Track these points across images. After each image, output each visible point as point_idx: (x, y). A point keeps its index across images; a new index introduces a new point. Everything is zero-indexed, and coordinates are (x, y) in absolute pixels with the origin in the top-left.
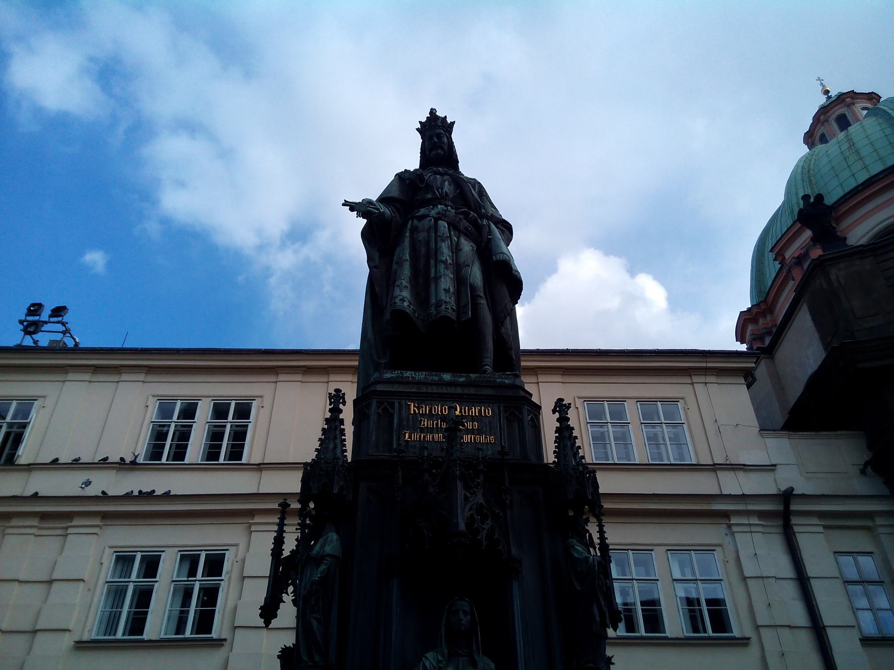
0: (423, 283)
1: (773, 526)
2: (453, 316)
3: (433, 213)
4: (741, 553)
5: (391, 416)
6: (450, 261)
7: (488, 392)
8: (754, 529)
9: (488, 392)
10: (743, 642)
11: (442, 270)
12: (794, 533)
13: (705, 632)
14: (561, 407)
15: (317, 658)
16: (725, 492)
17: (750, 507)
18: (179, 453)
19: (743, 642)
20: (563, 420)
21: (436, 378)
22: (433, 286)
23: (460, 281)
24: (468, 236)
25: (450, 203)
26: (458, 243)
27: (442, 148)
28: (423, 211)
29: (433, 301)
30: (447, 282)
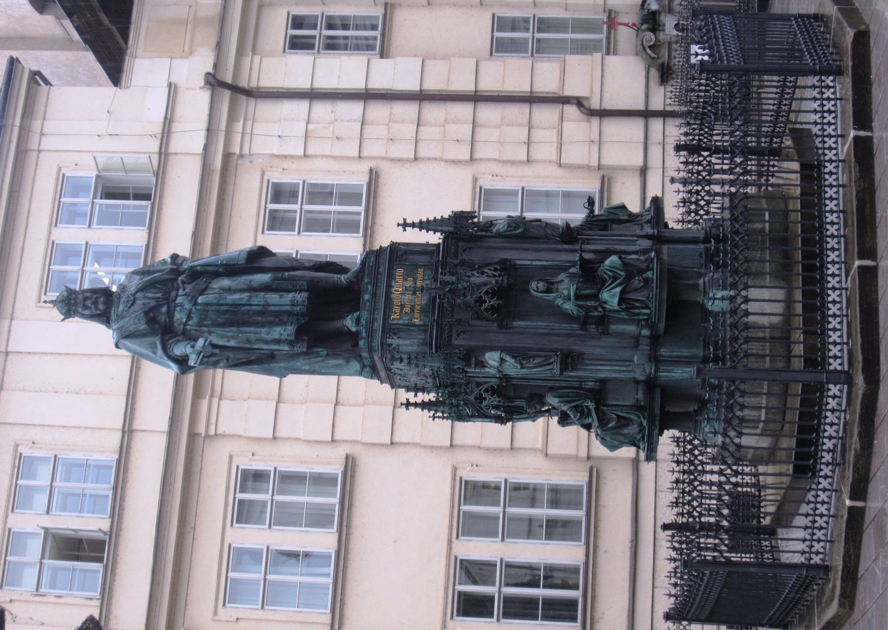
1: (247, 107)
2: (305, 295)
3: (188, 306)
4: (275, 152)
6: (247, 294)
8: (248, 130)
10: (374, 177)
12: (258, 88)
13: (360, 214)
14: (405, 225)
15: (552, 360)
16: (199, 149)
17: (223, 126)
19: (374, 177)
20: (413, 225)
22: (272, 308)
23: (266, 288)
25: (174, 294)
27: (97, 298)
30: (273, 298)
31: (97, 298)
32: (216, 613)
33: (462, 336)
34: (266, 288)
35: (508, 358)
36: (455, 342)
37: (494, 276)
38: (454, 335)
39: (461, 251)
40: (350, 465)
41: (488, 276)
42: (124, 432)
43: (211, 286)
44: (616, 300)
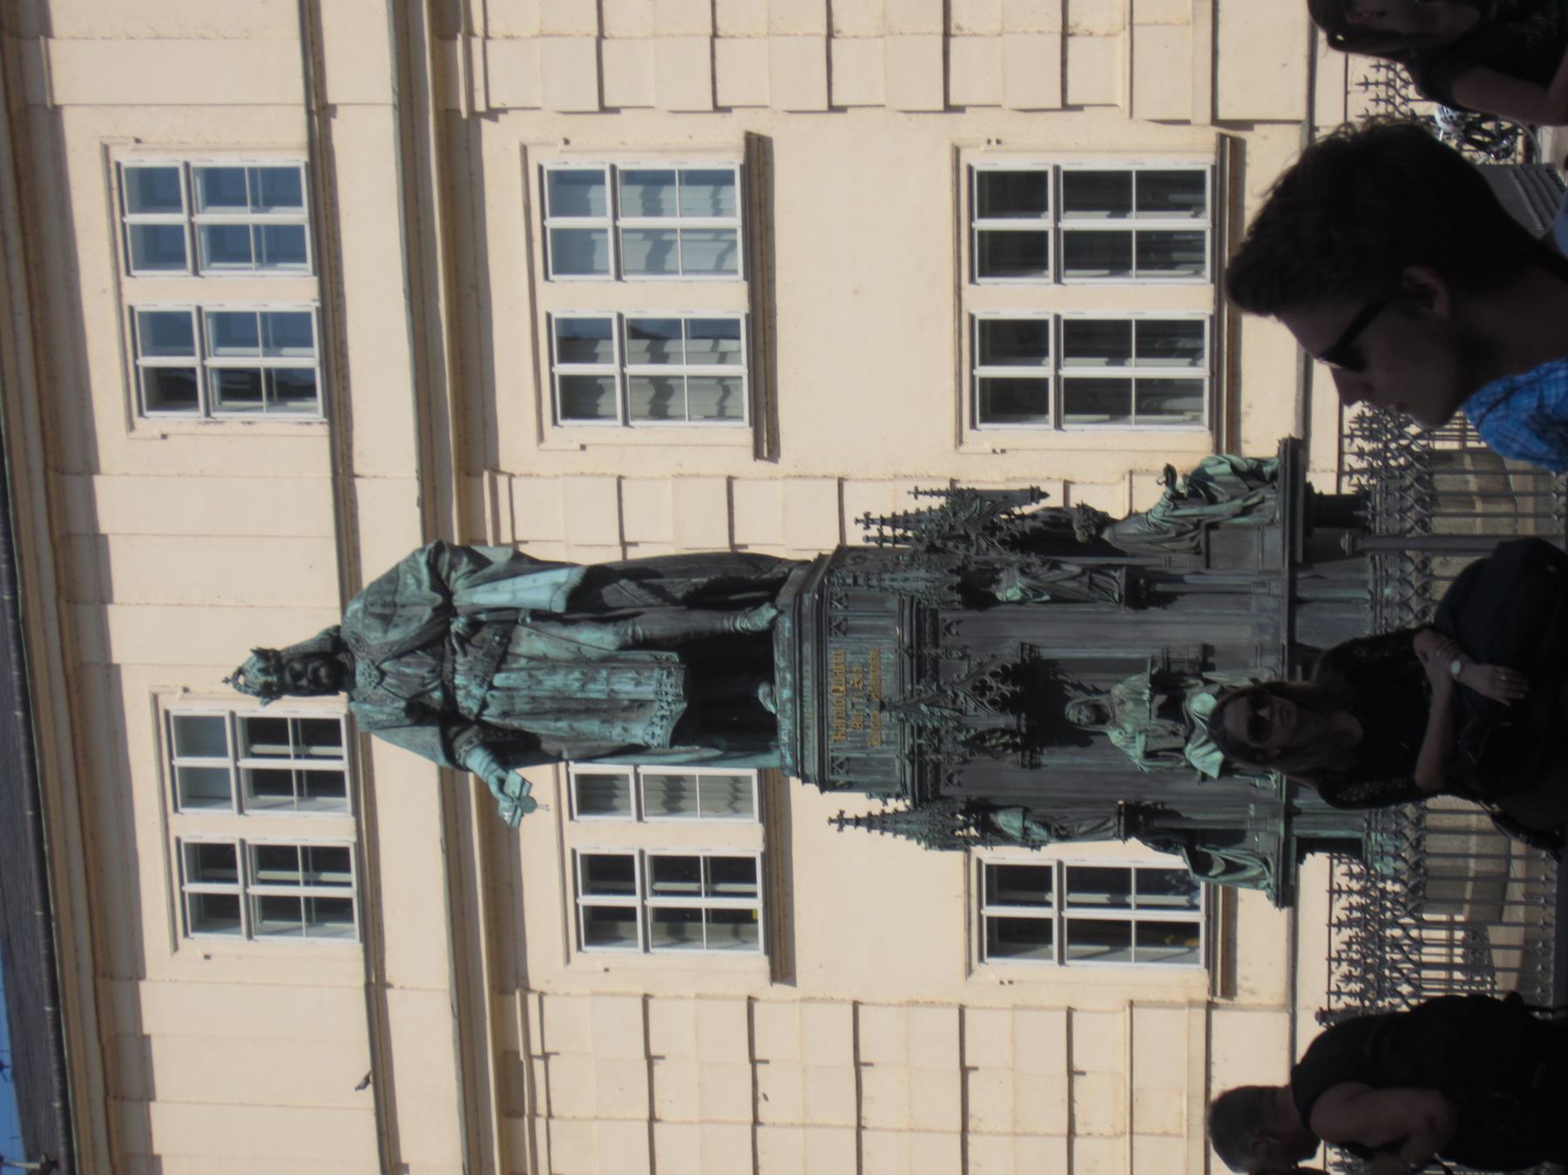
0: (610, 709)
3: (477, 692)
5: (848, 759)
6: (577, 674)
7: (808, 649)
9: (808, 649)
11: (599, 687)
18: (327, 859)
21: (789, 706)
22: (624, 696)
24: (507, 639)
25: (447, 667)
26: (531, 658)
27: (316, 671)
28: (467, 703)
29: (652, 697)
30: (625, 686)
31: (316, 671)
32: (541, 437)
33: (955, 780)
34: (606, 660)
35: (1035, 828)
36: (944, 791)
37: (1004, 704)
38: (943, 778)
39: (942, 627)
40: (758, 151)
41: (992, 702)
42: (309, 112)
43: (511, 649)
44: (1214, 773)
